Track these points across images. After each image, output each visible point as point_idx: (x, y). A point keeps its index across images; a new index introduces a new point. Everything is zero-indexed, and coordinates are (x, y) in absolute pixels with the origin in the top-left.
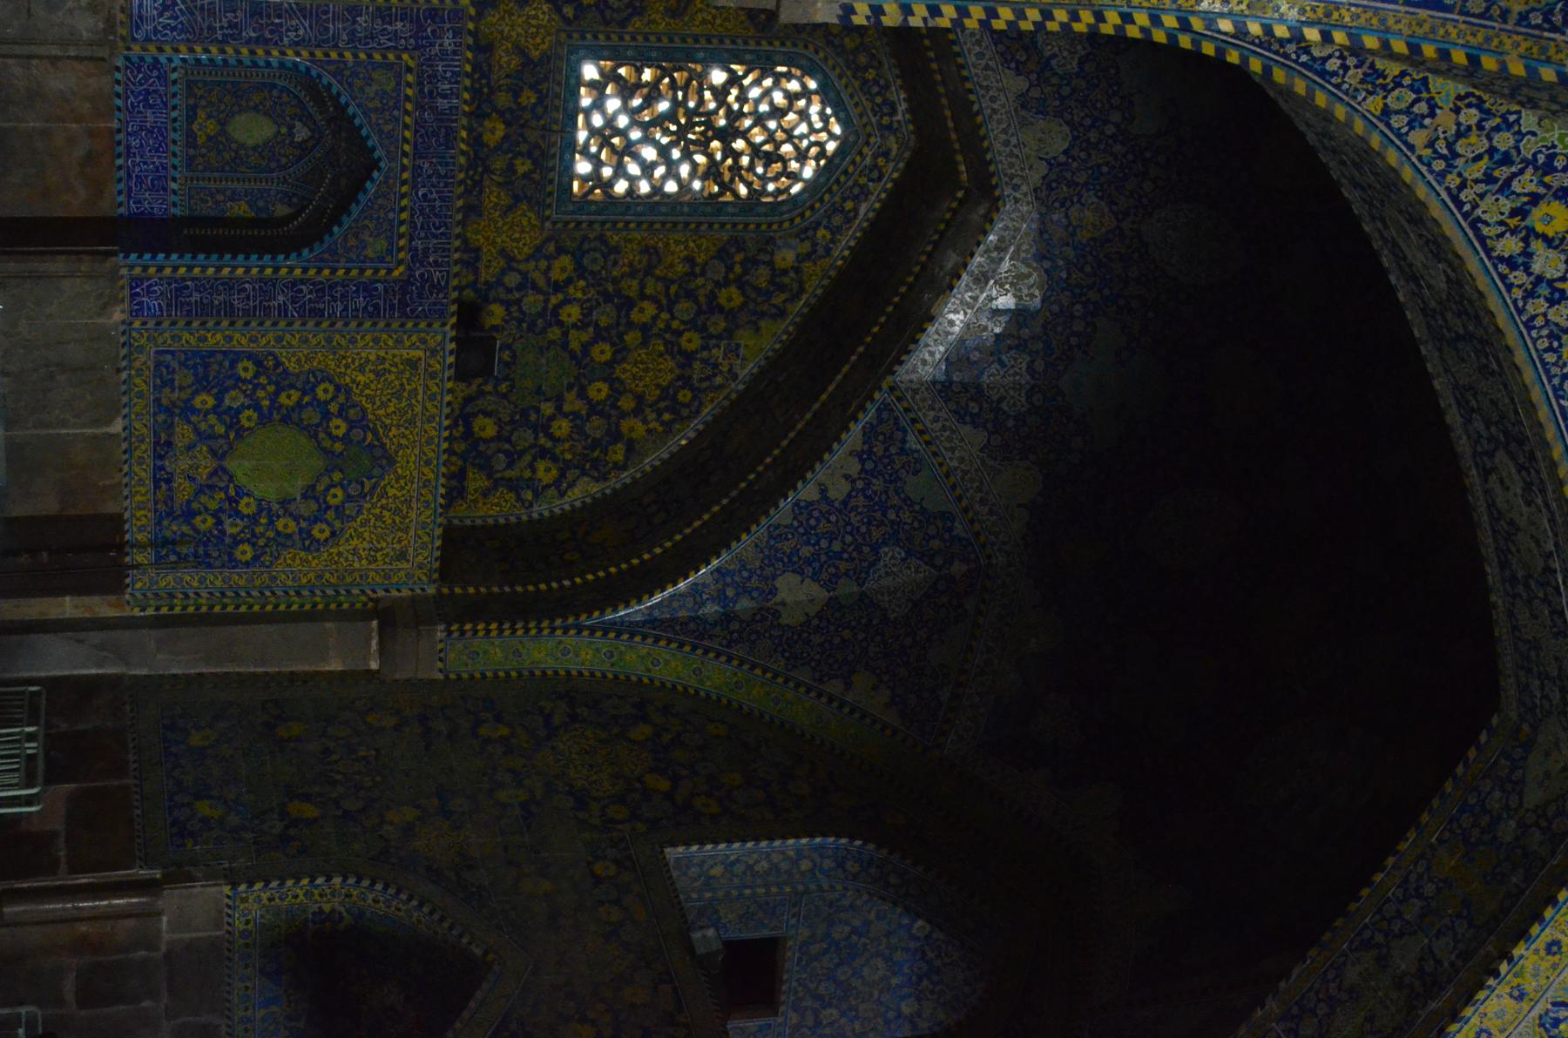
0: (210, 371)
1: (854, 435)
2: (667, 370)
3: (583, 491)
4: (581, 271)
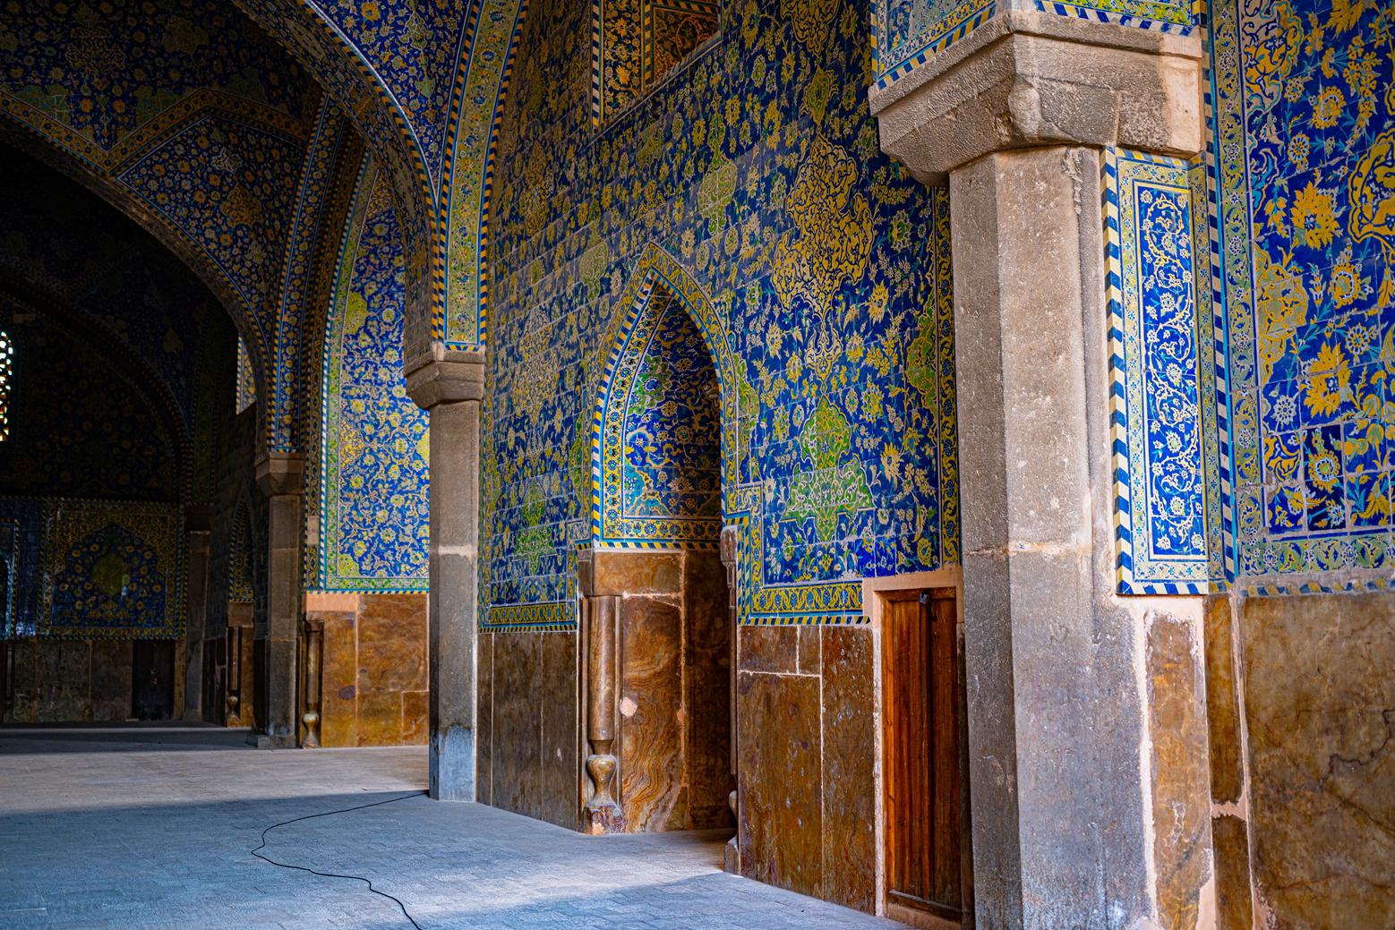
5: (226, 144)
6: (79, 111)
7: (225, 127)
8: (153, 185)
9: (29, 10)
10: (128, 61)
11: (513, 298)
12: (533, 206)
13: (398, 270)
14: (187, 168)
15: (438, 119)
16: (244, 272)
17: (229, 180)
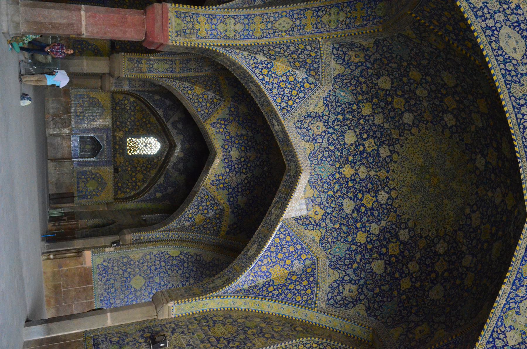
0: (84, 173)
1: (163, 175)
2: (142, 176)
3: (133, 193)
4: (130, 164)
5: (216, 214)
6: (219, 176)
8: (202, 196)
11: (190, 327)
12: (219, 330)
13: (188, 264)
14: (208, 204)
15: (238, 292)
16: (182, 221)
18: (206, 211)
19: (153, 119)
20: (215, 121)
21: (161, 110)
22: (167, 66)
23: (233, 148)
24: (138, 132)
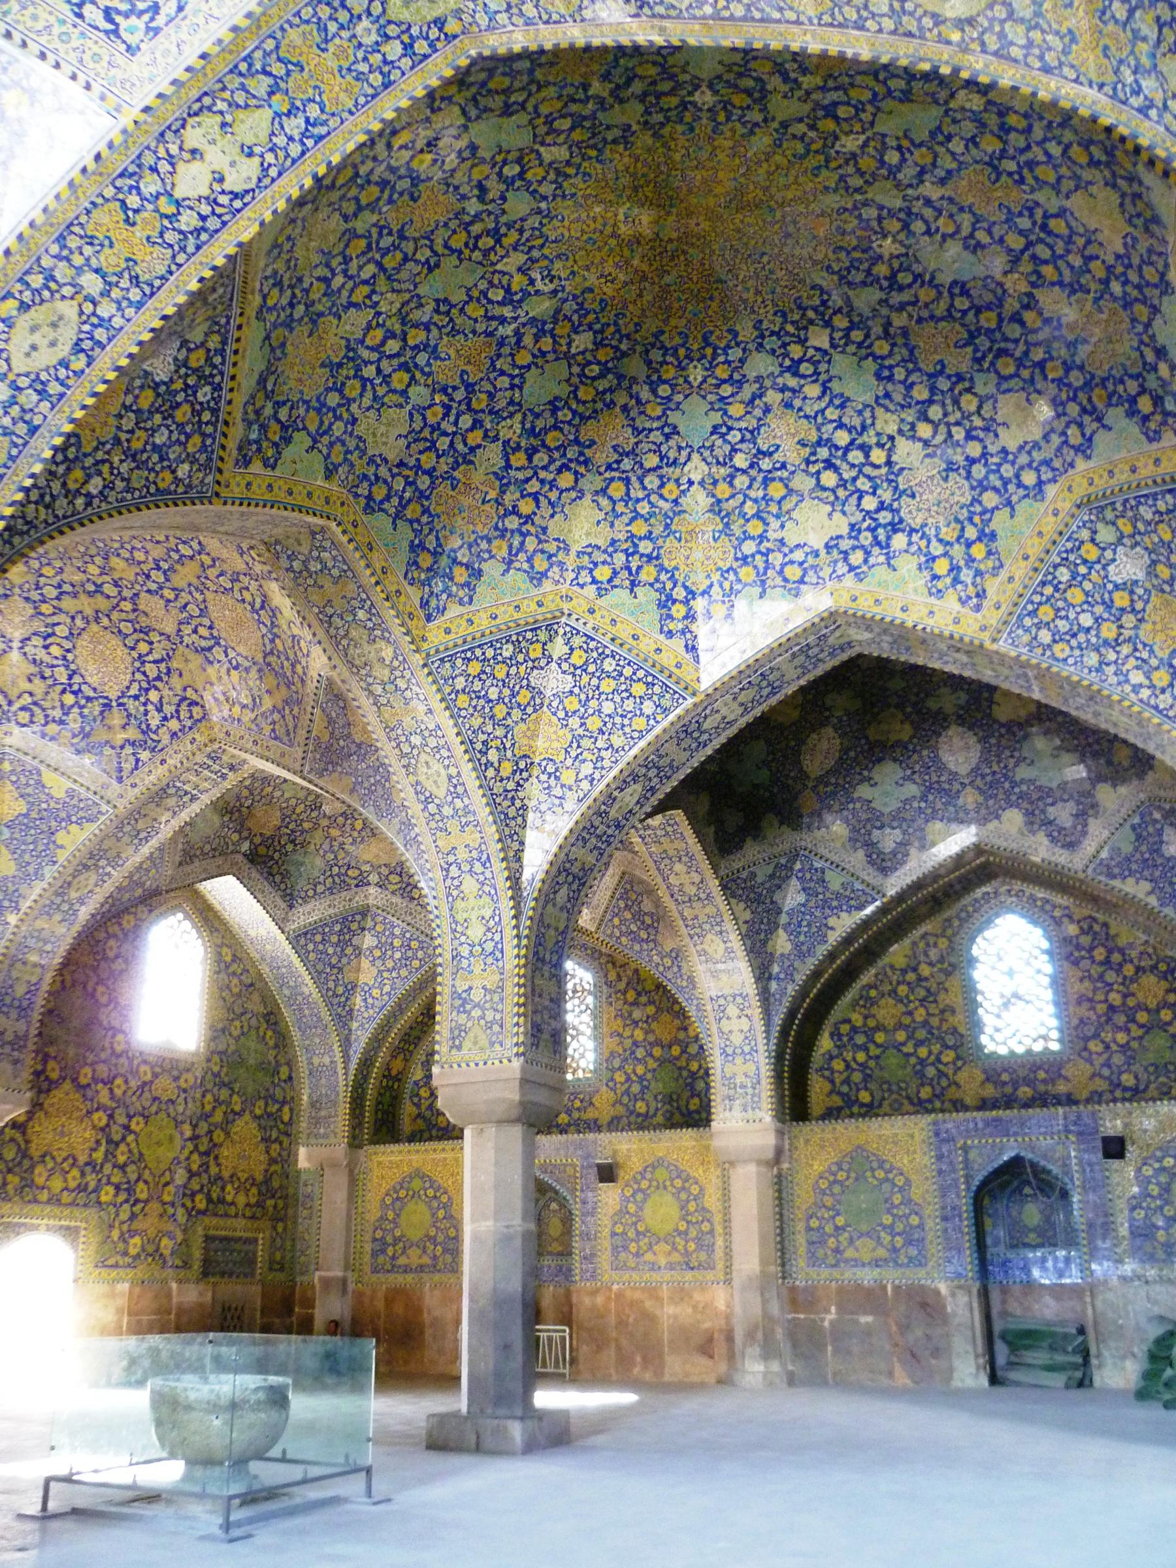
4: (1096, 1036)
6: (935, 577)
7: (1109, 515)
8: (1045, 636)
9: (846, 476)
10: (973, 488)
17: (1140, 591)
18: (1121, 600)
19: (897, 953)
20: (678, 644)
21: (832, 922)
22: (470, 885)
23: (792, 535)
24: (953, 1012)
